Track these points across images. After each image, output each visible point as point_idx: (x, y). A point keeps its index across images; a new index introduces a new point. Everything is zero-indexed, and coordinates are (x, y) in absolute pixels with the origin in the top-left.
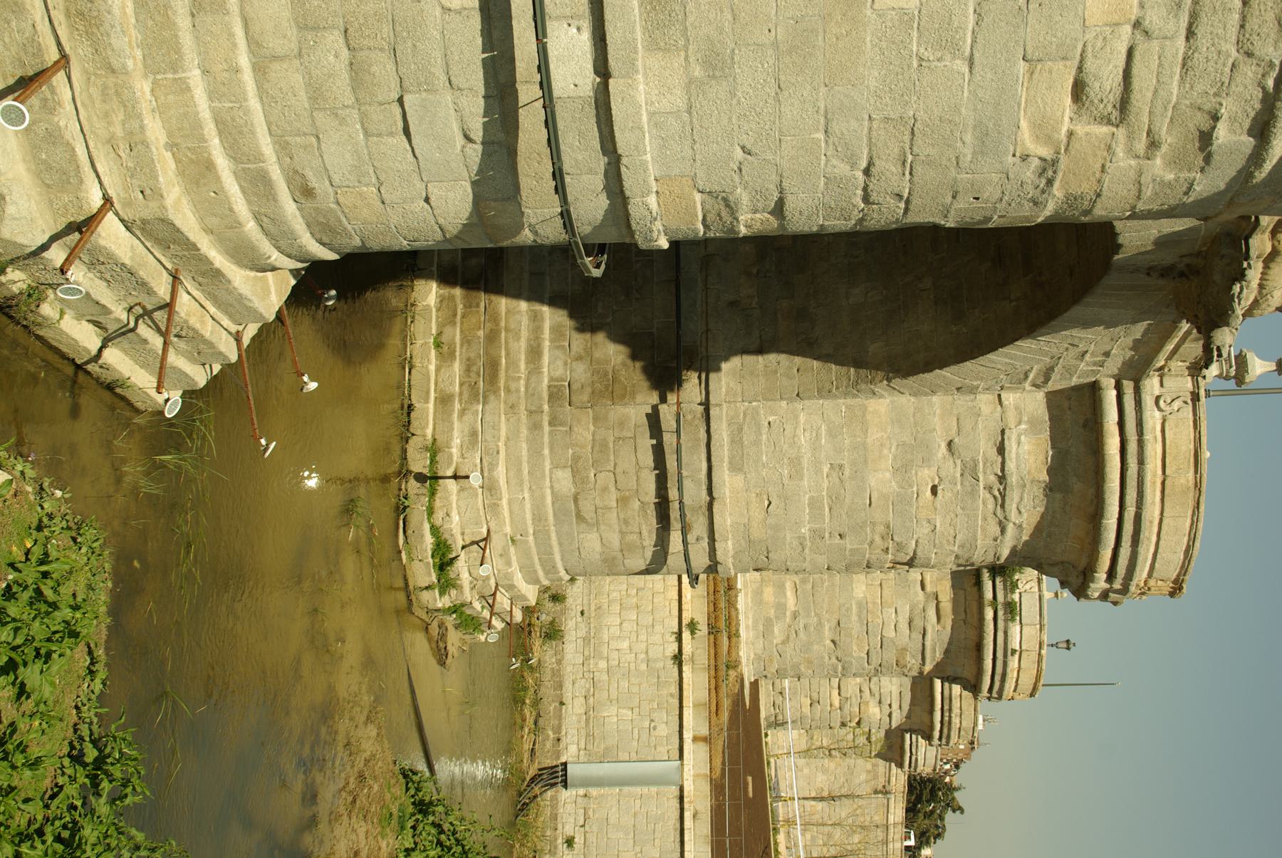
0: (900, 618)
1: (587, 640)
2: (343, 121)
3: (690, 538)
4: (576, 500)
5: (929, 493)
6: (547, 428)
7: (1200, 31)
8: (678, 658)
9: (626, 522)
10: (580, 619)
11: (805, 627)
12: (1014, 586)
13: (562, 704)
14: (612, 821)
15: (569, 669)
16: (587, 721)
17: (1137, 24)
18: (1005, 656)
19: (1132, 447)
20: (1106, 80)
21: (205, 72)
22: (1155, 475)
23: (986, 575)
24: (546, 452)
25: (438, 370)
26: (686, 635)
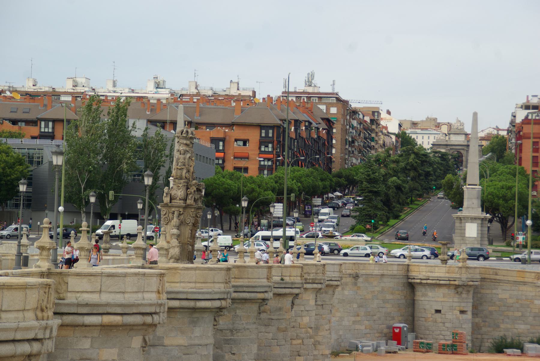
0: (264, 330)
18: (283, 283)
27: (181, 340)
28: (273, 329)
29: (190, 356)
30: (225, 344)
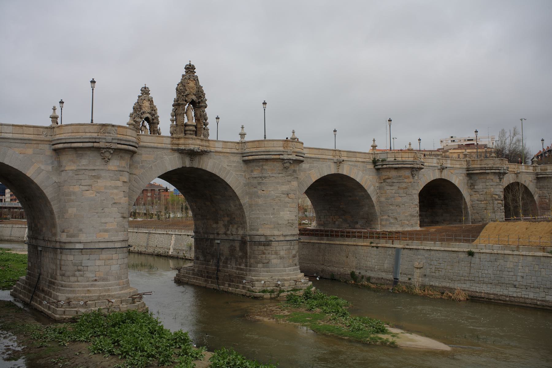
0: (389, 189)
1: (371, 271)
2: (85, 273)
3: (274, 240)
4: (264, 263)
5: (263, 192)
6: (252, 268)
7: (81, 179)
8: (377, 247)
9: (269, 253)
10: (367, 272)
11: (392, 214)
12: (378, 160)
13: (382, 278)
14: (407, 268)
15: (376, 275)
16: (387, 272)
17: (80, 185)
18: (396, 161)
19: (251, 154)
20: (86, 188)
21: (78, 288)
22: (256, 150)
23: (376, 167)
24: (254, 269)
25: (240, 289)
26: (373, 245)
27: (74, 167)
28: (395, 188)
29: (80, 176)
30: (259, 185)
